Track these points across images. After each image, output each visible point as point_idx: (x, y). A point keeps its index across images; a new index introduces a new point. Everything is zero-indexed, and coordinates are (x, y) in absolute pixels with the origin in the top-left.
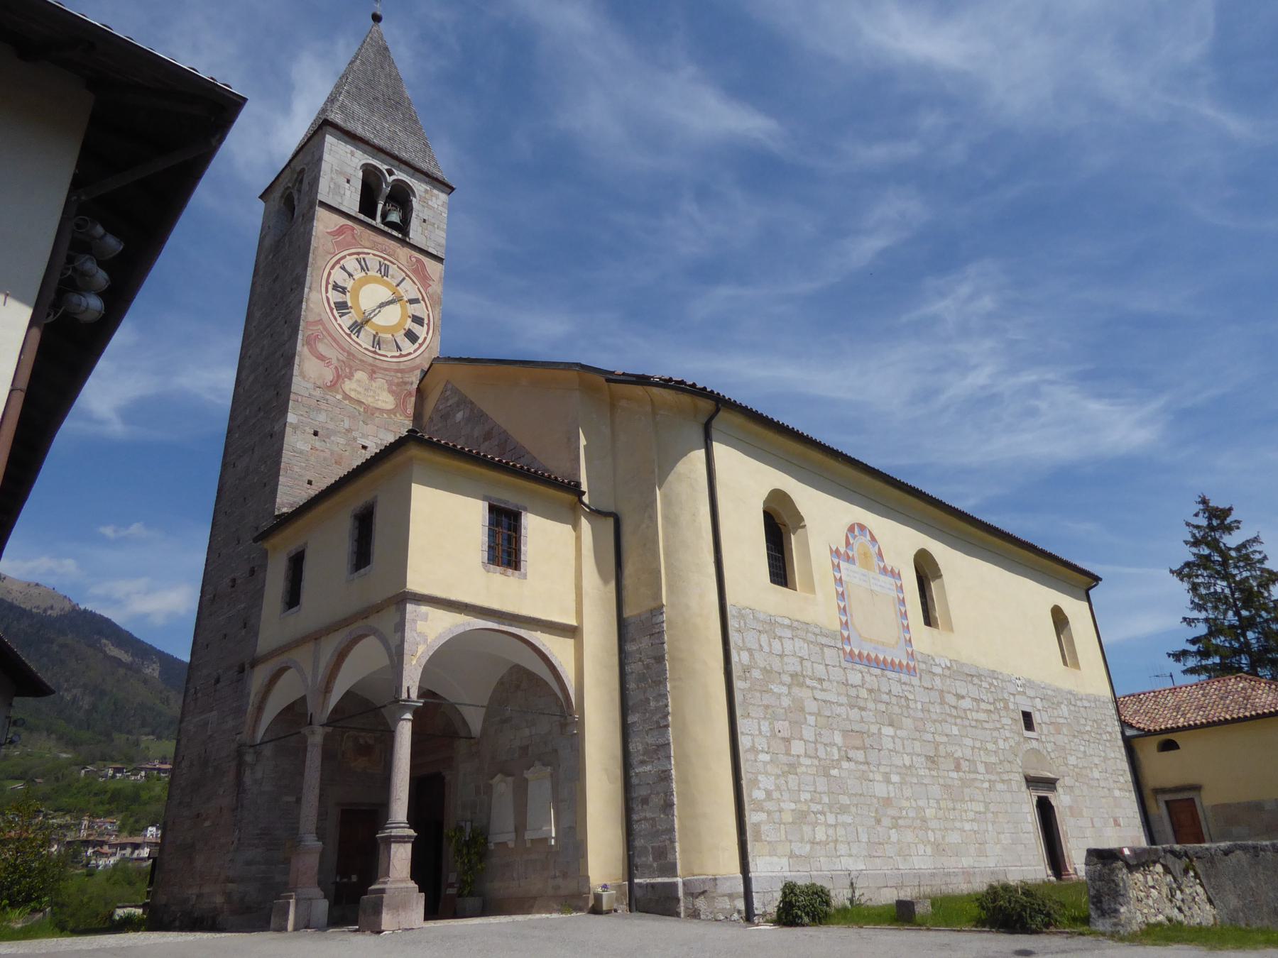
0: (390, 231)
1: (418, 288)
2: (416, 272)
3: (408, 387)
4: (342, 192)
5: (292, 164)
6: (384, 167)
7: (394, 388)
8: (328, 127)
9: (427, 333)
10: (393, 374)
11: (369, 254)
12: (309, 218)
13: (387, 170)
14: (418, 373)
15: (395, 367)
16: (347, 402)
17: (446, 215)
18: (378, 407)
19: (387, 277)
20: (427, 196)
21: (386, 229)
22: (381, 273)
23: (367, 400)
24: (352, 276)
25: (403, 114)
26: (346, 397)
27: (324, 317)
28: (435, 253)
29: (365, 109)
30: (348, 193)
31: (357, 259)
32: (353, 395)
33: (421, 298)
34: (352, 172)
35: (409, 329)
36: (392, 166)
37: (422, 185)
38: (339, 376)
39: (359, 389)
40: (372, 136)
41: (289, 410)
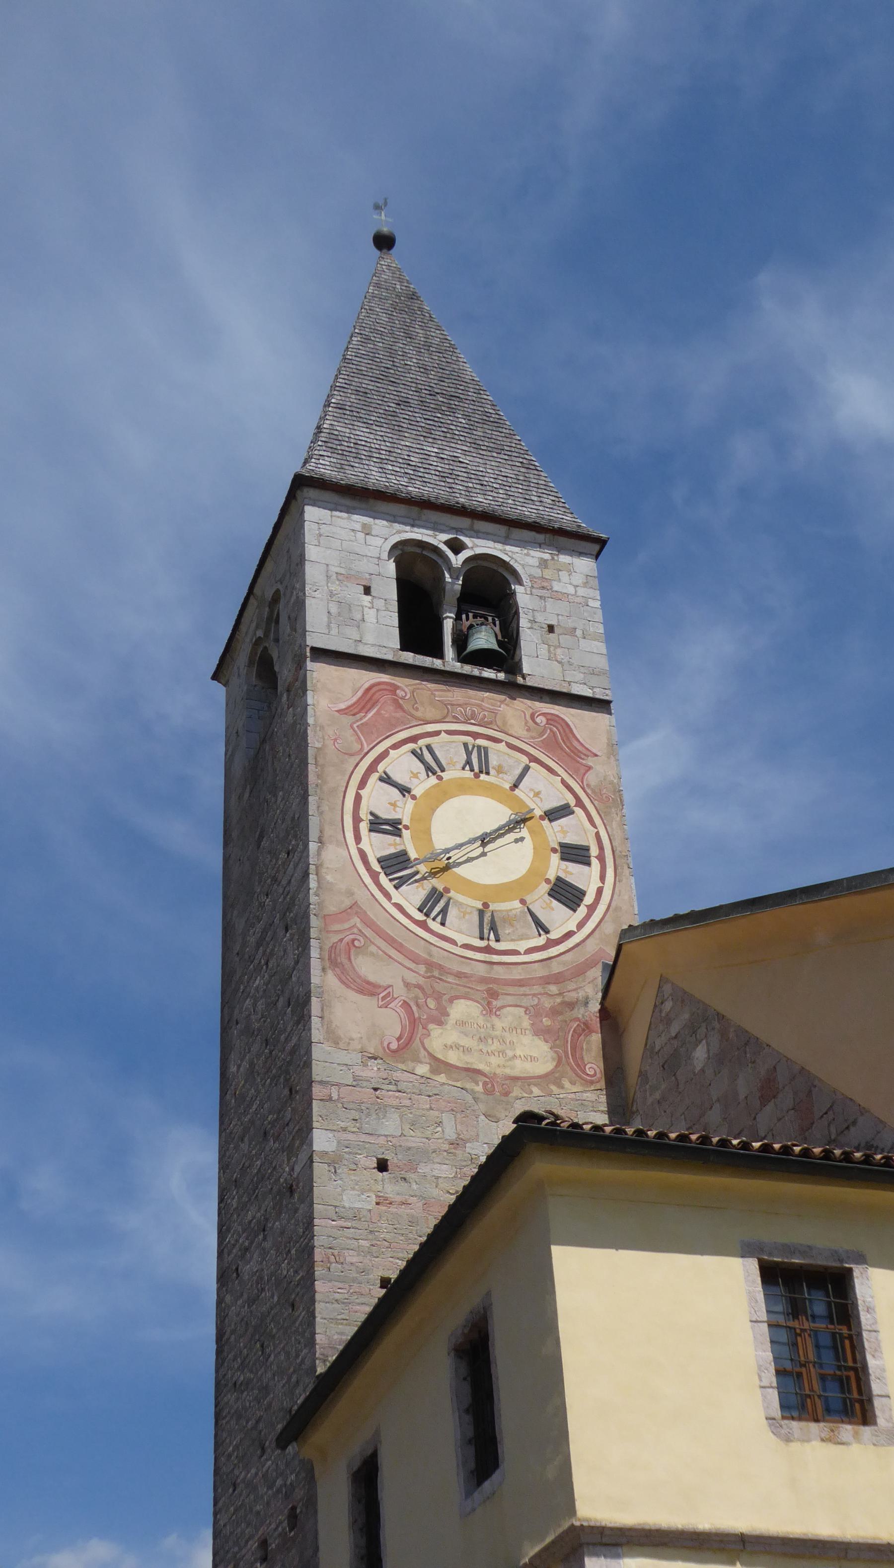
0: (476, 671)
1: (563, 782)
2: (550, 746)
3: (579, 1012)
4: (358, 617)
5: (257, 590)
6: (438, 539)
7: (546, 1021)
8: (305, 490)
9: (602, 878)
10: (537, 989)
11: (437, 733)
12: (299, 687)
13: (447, 543)
14: (597, 976)
15: (540, 971)
16: (442, 1078)
17: (597, 604)
18: (516, 1073)
19: (488, 773)
20: (548, 574)
21: (467, 669)
22: (472, 770)
23: (489, 1064)
24: (408, 791)
25: (467, 417)
26: (439, 1065)
27: (361, 896)
28: (588, 693)
29: (381, 431)
30: (370, 615)
31: (414, 752)
32: (453, 1058)
33: (572, 802)
34: (373, 569)
35: (559, 879)
36: (459, 530)
37: (532, 553)
38: (414, 1022)
39: (466, 1042)
40: (404, 481)
41: (315, 1124)
